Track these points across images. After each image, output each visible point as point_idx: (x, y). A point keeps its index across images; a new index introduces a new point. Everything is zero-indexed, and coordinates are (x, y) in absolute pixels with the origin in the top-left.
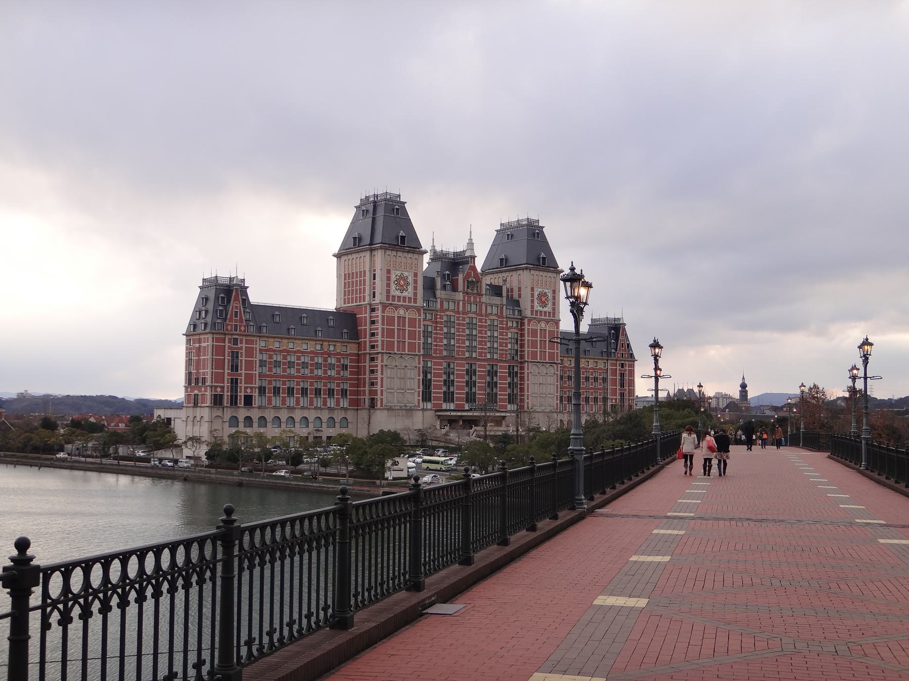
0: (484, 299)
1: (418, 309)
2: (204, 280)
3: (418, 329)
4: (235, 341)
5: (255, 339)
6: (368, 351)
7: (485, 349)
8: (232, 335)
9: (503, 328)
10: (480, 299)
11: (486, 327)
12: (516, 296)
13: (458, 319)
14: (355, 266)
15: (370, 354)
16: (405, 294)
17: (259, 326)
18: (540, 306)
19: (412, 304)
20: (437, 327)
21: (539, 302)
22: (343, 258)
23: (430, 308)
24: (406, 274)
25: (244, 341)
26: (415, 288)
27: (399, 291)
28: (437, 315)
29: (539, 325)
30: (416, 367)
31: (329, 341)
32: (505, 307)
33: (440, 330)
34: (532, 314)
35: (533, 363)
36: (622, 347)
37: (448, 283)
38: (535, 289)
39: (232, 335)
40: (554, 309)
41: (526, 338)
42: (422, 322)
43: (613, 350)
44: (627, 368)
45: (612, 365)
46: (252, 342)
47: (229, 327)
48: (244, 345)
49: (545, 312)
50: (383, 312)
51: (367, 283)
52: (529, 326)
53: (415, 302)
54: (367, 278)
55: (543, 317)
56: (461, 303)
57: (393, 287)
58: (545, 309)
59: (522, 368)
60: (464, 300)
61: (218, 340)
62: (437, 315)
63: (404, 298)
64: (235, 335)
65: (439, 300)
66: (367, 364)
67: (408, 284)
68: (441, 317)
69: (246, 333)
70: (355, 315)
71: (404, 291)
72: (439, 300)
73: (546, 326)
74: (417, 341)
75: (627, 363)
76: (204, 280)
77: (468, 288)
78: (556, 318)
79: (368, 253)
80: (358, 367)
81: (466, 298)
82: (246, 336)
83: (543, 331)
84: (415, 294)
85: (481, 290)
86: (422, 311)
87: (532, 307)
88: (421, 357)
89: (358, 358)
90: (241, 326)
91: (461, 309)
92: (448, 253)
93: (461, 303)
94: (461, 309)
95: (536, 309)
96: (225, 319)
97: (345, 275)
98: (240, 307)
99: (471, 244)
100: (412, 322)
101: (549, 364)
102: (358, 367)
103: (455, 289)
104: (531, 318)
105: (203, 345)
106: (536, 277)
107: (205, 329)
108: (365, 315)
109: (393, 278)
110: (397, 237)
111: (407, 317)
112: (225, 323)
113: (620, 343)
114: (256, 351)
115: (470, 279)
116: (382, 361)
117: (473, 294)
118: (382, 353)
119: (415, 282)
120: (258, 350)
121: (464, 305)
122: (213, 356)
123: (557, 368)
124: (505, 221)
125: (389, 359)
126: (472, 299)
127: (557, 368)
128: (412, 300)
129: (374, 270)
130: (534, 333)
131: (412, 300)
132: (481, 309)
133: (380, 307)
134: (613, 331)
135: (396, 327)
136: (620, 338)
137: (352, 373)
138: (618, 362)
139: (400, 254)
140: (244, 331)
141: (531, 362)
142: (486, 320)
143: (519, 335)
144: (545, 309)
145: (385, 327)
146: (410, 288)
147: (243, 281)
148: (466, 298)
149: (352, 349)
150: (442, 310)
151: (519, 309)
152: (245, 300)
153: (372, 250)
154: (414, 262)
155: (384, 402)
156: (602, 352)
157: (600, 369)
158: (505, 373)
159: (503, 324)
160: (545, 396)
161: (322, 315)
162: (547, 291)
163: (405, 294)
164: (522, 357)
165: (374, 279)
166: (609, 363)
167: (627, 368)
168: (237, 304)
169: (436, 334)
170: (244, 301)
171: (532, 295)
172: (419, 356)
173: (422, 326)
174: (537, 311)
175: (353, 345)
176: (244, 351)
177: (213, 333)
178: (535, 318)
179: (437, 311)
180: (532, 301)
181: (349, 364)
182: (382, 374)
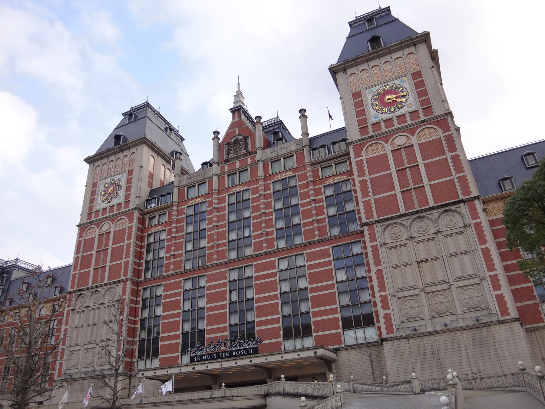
0: (259, 155)
18: (384, 113)
21: (379, 107)
35: (387, 223)
77: (228, 154)
78: (437, 111)
100: (119, 235)
101: (441, 210)
104: (360, 140)
111: (112, 230)
117: (238, 158)
125: (80, 299)
155: (64, 369)
160: (446, 286)
163: (115, 202)
174: (376, 125)
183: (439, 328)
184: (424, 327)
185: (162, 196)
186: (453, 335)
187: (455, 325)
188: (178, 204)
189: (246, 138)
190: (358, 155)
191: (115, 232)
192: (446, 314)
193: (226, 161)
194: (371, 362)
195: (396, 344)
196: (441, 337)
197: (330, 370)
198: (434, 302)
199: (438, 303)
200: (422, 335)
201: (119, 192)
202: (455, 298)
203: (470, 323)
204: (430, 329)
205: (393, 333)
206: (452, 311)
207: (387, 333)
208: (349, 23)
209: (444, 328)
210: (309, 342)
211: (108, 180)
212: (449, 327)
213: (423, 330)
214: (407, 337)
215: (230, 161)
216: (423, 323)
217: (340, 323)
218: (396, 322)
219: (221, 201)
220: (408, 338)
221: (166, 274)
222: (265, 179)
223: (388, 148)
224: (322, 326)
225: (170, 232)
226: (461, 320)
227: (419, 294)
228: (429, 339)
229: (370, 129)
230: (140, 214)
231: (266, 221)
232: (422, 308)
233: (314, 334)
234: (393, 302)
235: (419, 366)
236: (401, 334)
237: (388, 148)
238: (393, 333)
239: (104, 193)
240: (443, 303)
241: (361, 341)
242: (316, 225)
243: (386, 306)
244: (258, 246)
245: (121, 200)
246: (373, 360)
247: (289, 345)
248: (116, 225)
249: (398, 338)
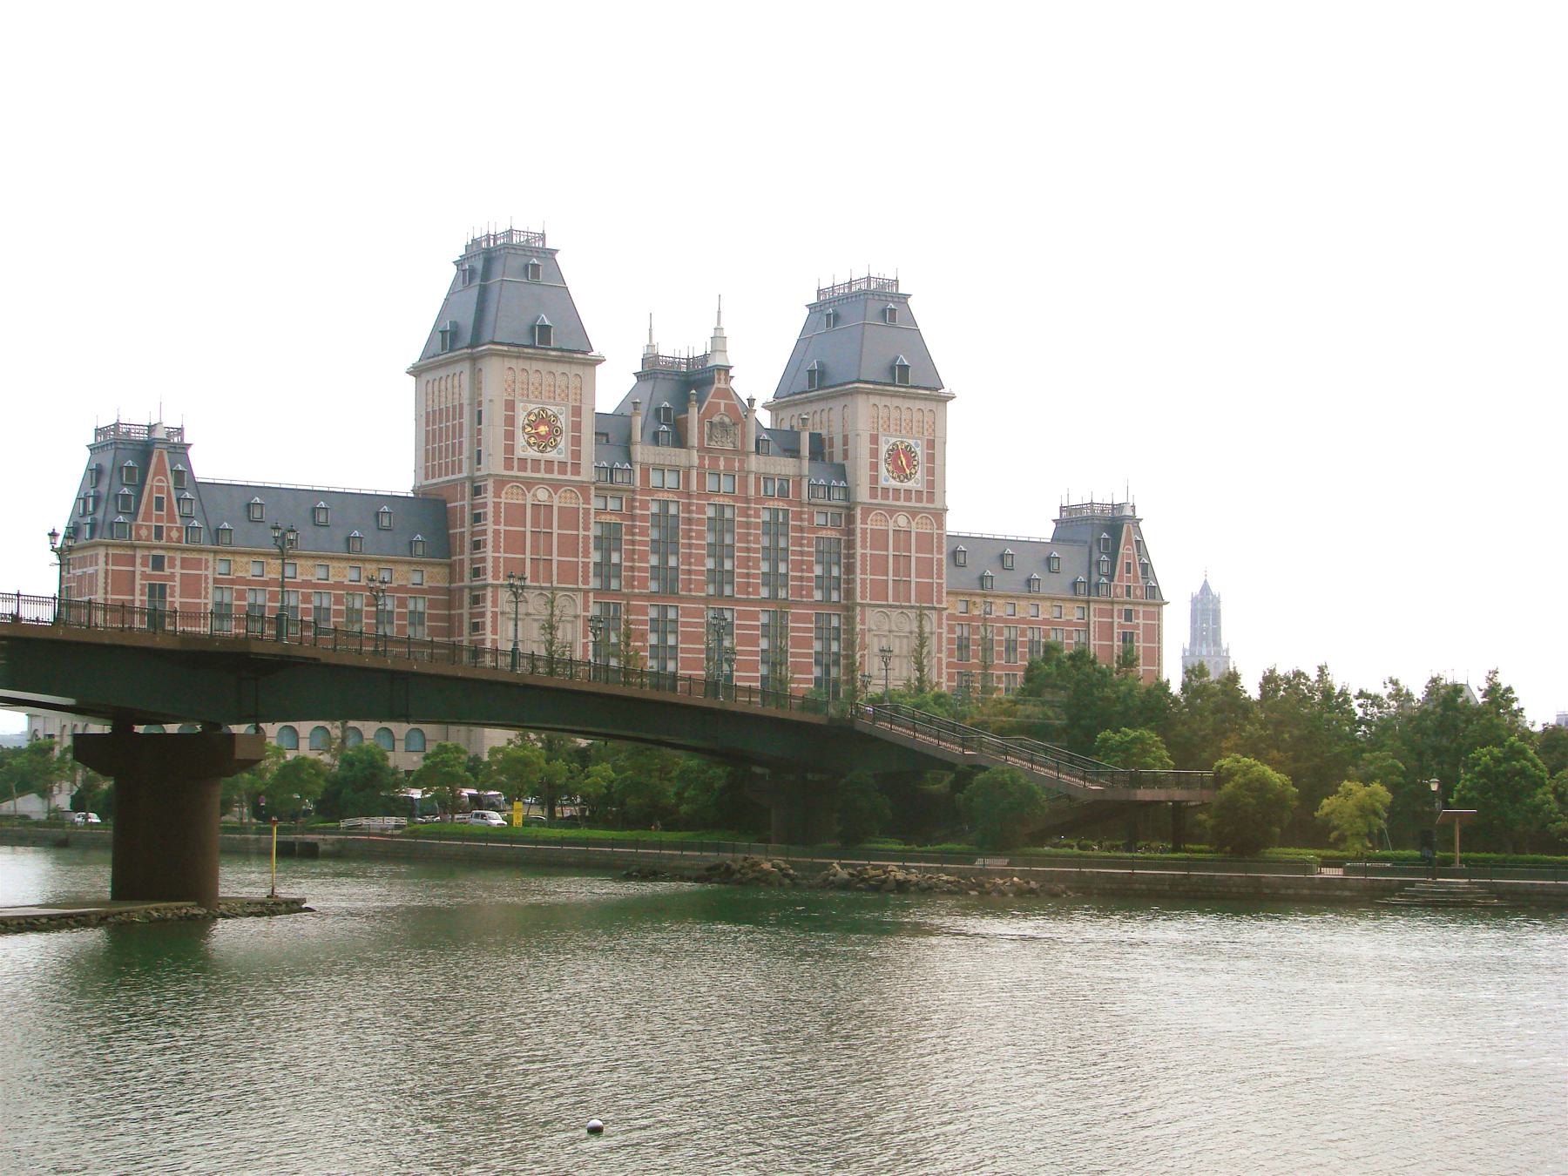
1: (583, 488)
2: (98, 431)
3: (582, 533)
4: (158, 563)
5: (204, 556)
6: (467, 582)
7: (755, 576)
8: (149, 548)
9: (801, 529)
10: (742, 462)
11: (756, 526)
12: (838, 459)
13: (688, 510)
14: (457, 390)
15: (471, 589)
16: (552, 455)
17: (213, 528)
19: (569, 477)
20: (634, 527)
21: (890, 468)
22: (429, 376)
24: (552, 409)
25: (178, 563)
26: (576, 441)
27: (536, 448)
28: (634, 500)
29: (891, 522)
30: (576, 617)
31: (378, 561)
33: (641, 534)
36: (1128, 571)
37: (665, 428)
38: (882, 439)
39: (149, 548)
40: (931, 484)
41: (859, 551)
42: (592, 516)
43: (1104, 580)
44: (1141, 621)
45: (1101, 613)
46: (197, 564)
47: (144, 533)
48: (178, 571)
49: (908, 492)
50: (497, 494)
51: (466, 433)
52: (864, 521)
53: (576, 471)
54: (466, 420)
55: (902, 503)
56: (694, 473)
57: (520, 440)
58: (910, 485)
59: (850, 620)
60: (701, 466)
61: (117, 560)
62: (634, 500)
63: (549, 463)
64: (155, 548)
65: (637, 469)
66: (465, 611)
67: (559, 432)
68: (645, 505)
69: (184, 544)
70: (444, 502)
71: (549, 449)
72: (637, 469)
73: (909, 522)
74: (581, 559)
75: (1141, 609)
76: (98, 431)
77: (710, 438)
78: (937, 505)
79: (465, 367)
80: (450, 618)
81: (707, 462)
82: (183, 550)
83: (902, 535)
84: (576, 455)
85: (743, 443)
86: (593, 492)
88: (591, 595)
89: (450, 597)
90: (170, 529)
91: (694, 486)
92: (675, 362)
93: (694, 473)
94: (694, 486)
95: (882, 483)
96: (135, 515)
97: (427, 414)
98: (168, 487)
99: (718, 339)
102: (450, 618)
103: (680, 441)
105: (90, 570)
106: (883, 413)
107: (91, 538)
108: (463, 503)
109: (521, 418)
110: (533, 328)
112: (134, 523)
113: (1122, 562)
114: (207, 583)
115: (716, 419)
116: (495, 604)
118: (495, 587)
119: (577, 427)
120: (211, 581)
121: (701, 477)
122: (106, 593)
123: (940, 619)
124: (826, 284)
126: (722, 463)
127: (940, 619)
128: (569, 468)
129: (480, 404)
130: (879, 538)
131: (569, 468)
132: (745, 486)
133: (490, 484)
134: (1105, 535)
135: (529, 528)
136: (1121, 550)
137: (433, 631)
138: (1116, 607)
140: (179, 541)
141: (870, 605)
142: (757, 511)
143: (843, 544)
144: (910, 485)
145: (502, 528)
146: (563, 442)
147: (180, 431)
148: (707, 462)
149: (433, 577)
150: (647, 490)
151: (842, 483)
152: (183, 477)
153: (474, 359)
154: (574, 382)
156: (1075, 584)
157: (1069, 623)
158: (809, 630)
159: (802, 520)
161: (372, 505)
162: (912, 442)
163: (552, 455)
164: (850, 593)
165: (480, 423)
166: (1092, 609)
167: (1141, 621)
168: (160, 481)
169: (690, 546)
170: (179, 475)
171: (874, 453)
172: (586, 592)
173: (592, 525)
175: (436, 570)
176: (177, 583)
177: (107, 546)
179: (634, 491)
181: (427, 611)
182: (495, 632)
201: (558, 439)
211: (534, 406)
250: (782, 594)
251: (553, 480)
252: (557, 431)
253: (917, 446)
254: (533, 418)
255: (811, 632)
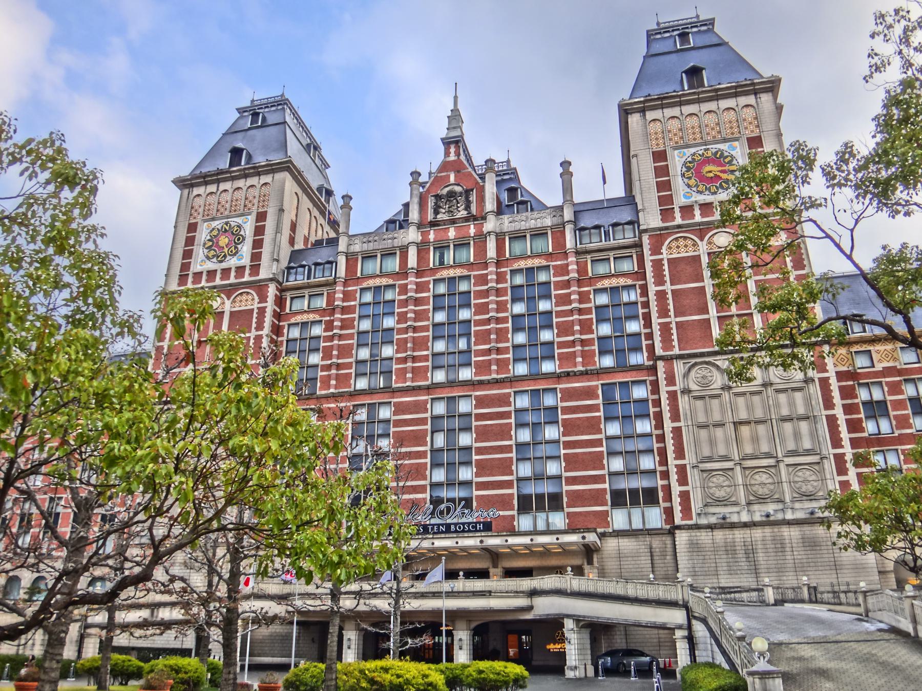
0: (490, 225)
16: (232, 262)
18: (701, 192)
21: (692, 182)
23: (312, 280)
32: (569, 229)
34: (667, 214)
35: (693, 361)
77: (436, 212)
87: (666, 202)
104: (660, 229)
117: (453, 222)
139: (223, 186)
160: (771, 462)
163: (232, 262)
174: (687, 210)
178: (679, 226)
180: (664, 186)
183: (757, 518)
184: (736, 515)
185: (316, 264)
186: (776, 530)
187: (780, 516)
188: (346, 283)
189: (467, 192)
190: (656, 250)
191: (232, 314)
192: (768, 500)
193: (433, 224)
194: (652, 556)
195: (693, 534)
196: (760, 531)
197: (590, 562)
198: (753, 482)
199: (759, 484)
200: (733, 526)
201: (239, 246)
202: (784, 479)
203: (800, 515)
204: (745, 518)
205: (691, 519)
206: (776, 496)
207: (682, 519)
208: (648, 31)
209: (764, 519)
210: (558, 520)
211: (217, 222)
212: (772, 518)
213: (734, 519)
214: (711, 527)
215: (438, 225)
216: (735, 509)
217: (608, 497)
218: (696, 505)
219: (421, 287)
220: (712, 528)
221: (324, 392)
222: (498, 264)
223: (703, 248)
224: (578, 498)
225: (329, 326)
226: (790, 511)
227: (732, 469)
228: (742, 532)
229: (678, 215)
230: (277, 289)
231: (499, 332)
232: (735, 489)
233: (566, 510)
234: (693, 476)
235: (725, 568)
236: (703, 521)
237: (703, 248)
238: (691, 519)
239: (211, 243)
240: (765, 484)
241: (637, 524)
242: (579, 348)
243: (683, 481)
244: (483, 368)
245: (243, 261)
246: (655, 554)
247: (525, 522)
248: (234, 301)
249: (697, 527)
250: (548, 367)
251: (230, 285)
252: (239, 239)
253: (734, 148)
254: (215, 233)
255: (599, 411)
